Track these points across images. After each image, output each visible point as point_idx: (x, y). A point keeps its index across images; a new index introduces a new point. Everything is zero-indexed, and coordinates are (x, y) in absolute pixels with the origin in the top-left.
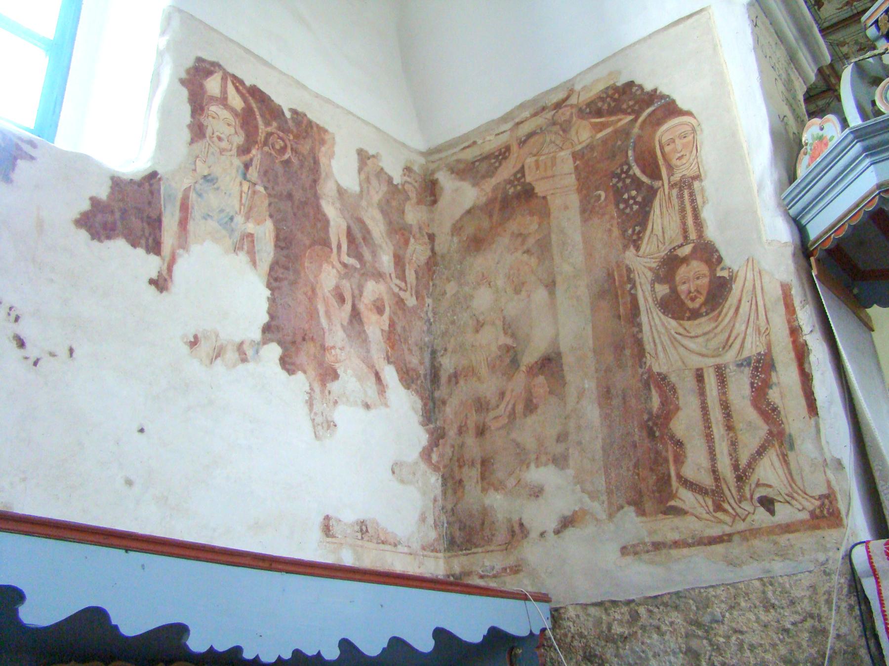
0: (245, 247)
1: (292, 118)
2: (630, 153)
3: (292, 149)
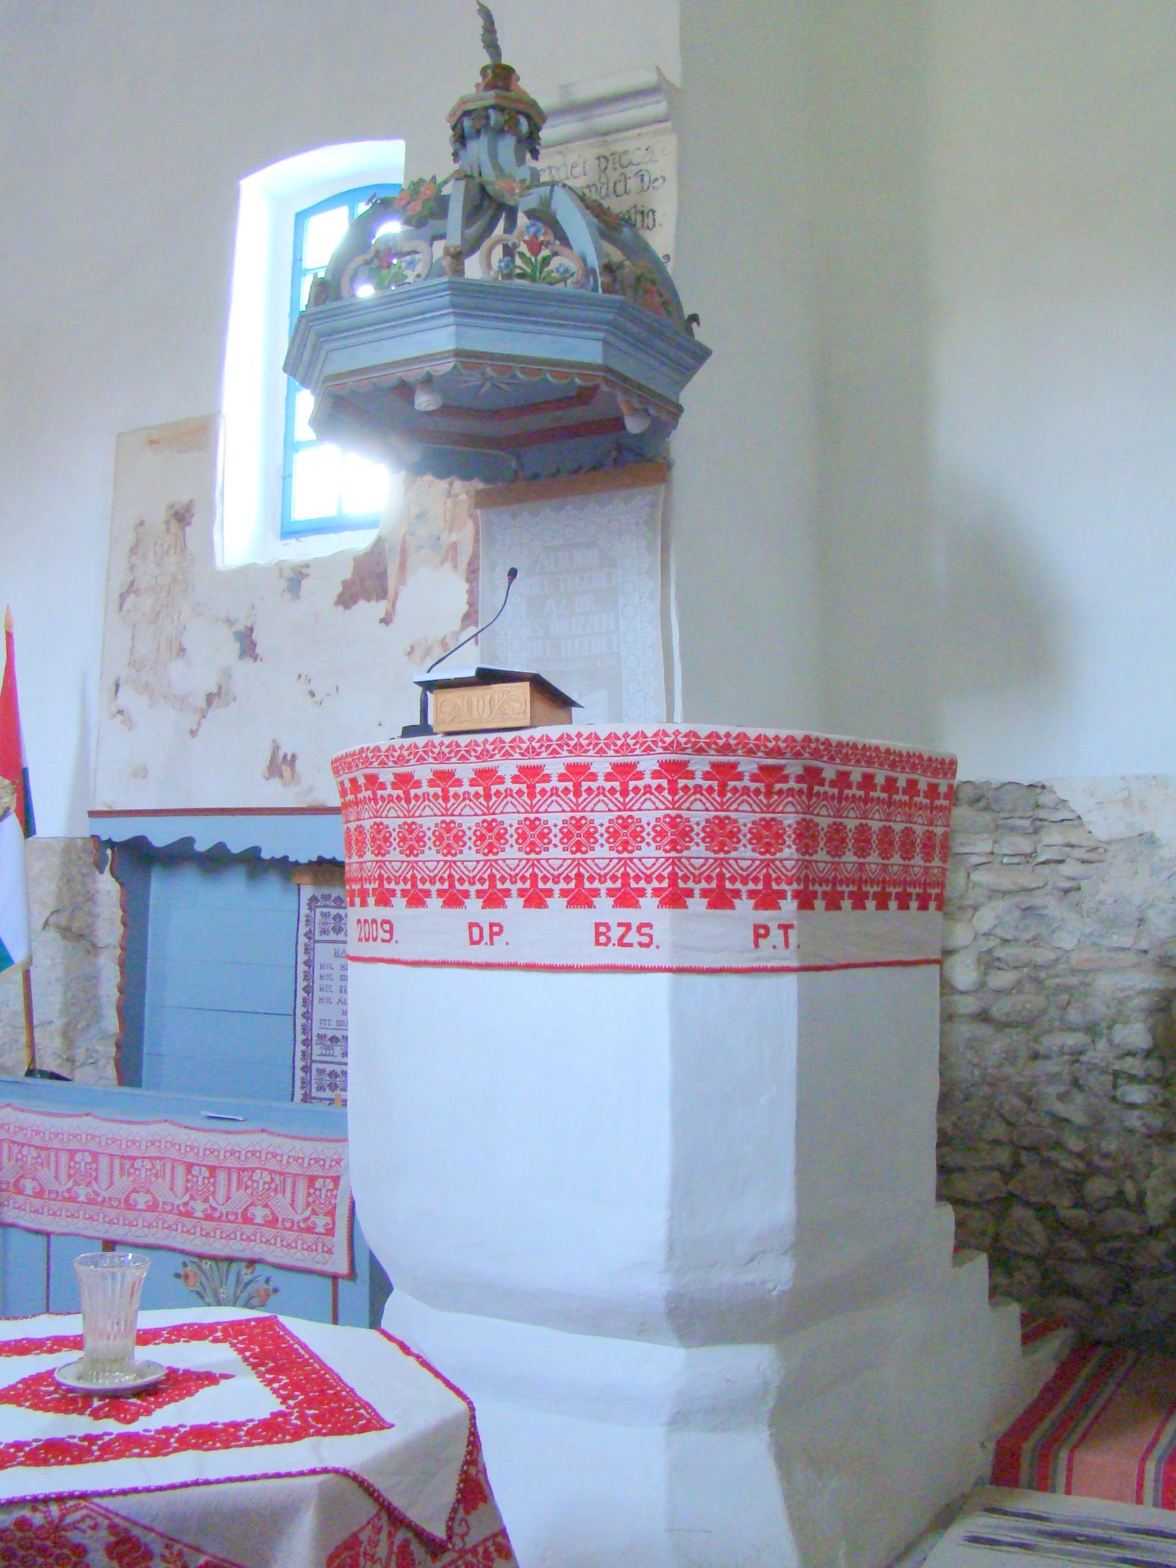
0: (450, 557)
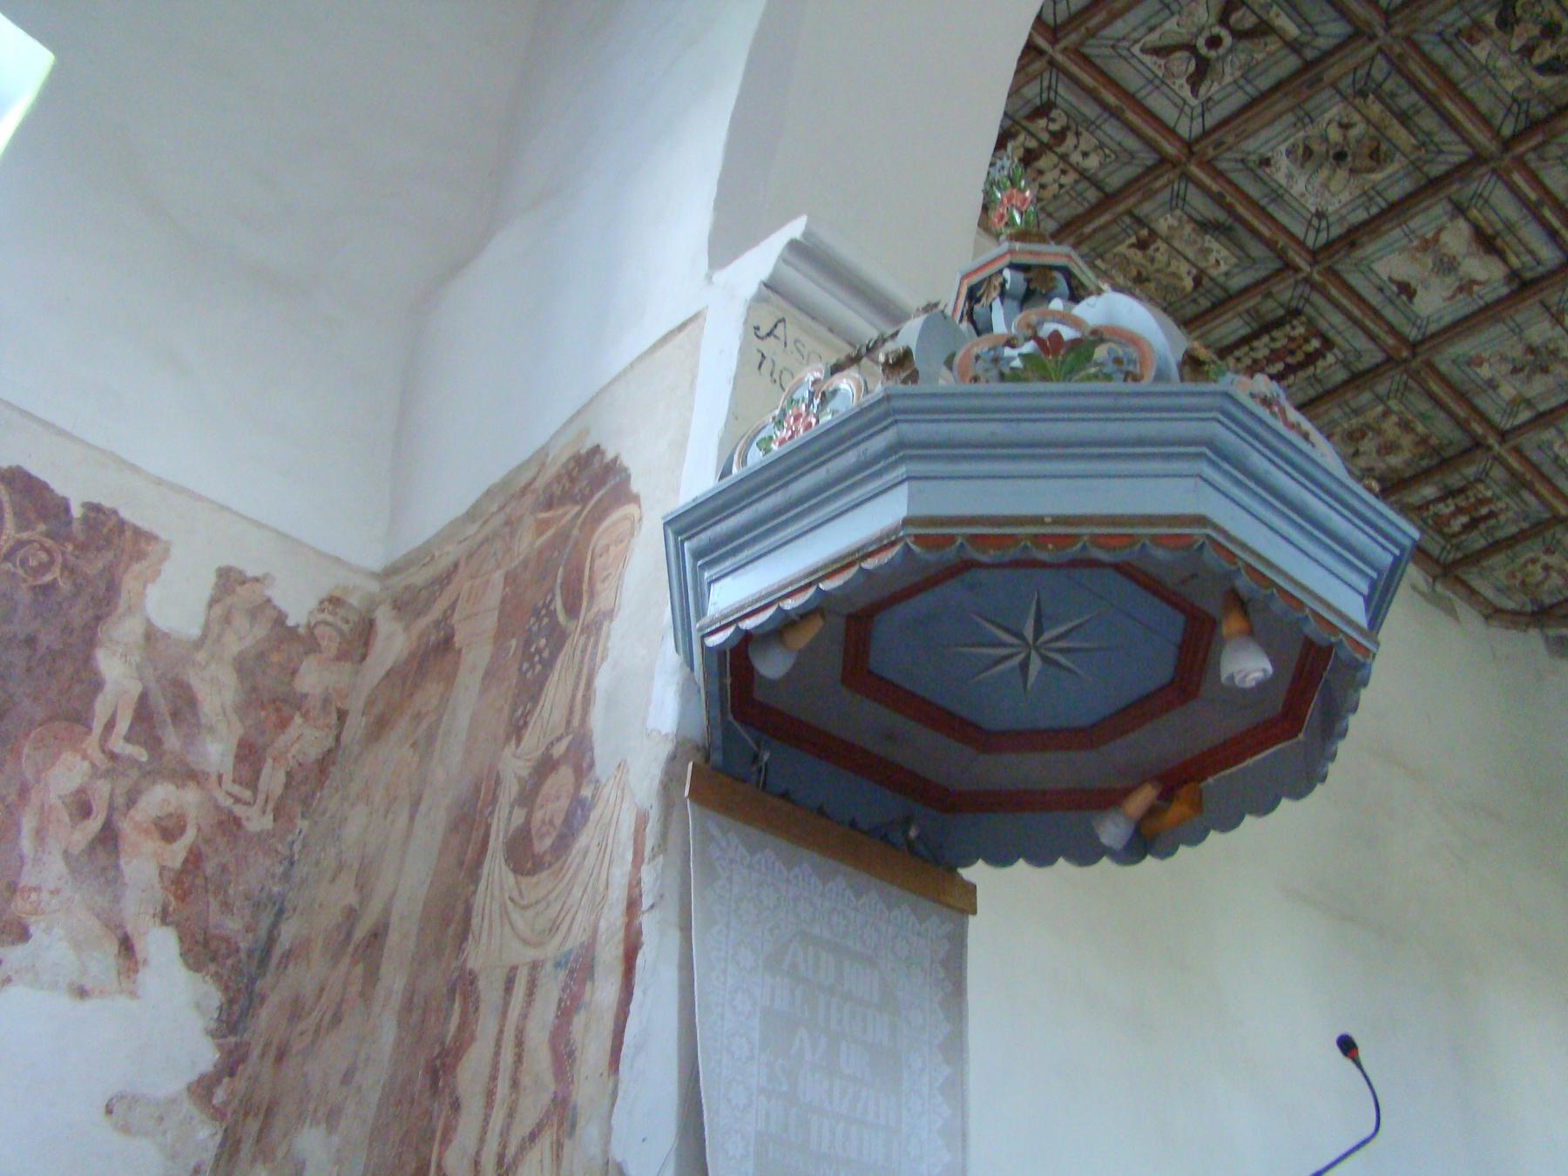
1: (85, 519)
3: (65, 566)
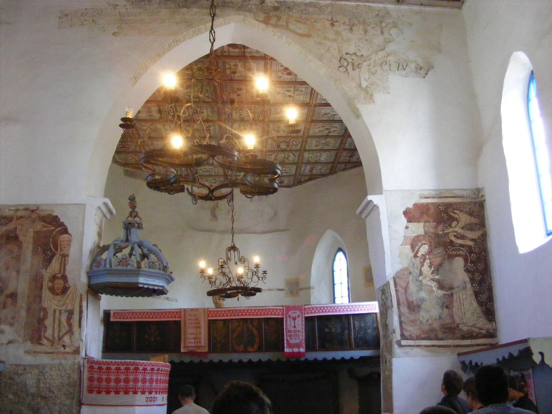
2: (51, 239)
